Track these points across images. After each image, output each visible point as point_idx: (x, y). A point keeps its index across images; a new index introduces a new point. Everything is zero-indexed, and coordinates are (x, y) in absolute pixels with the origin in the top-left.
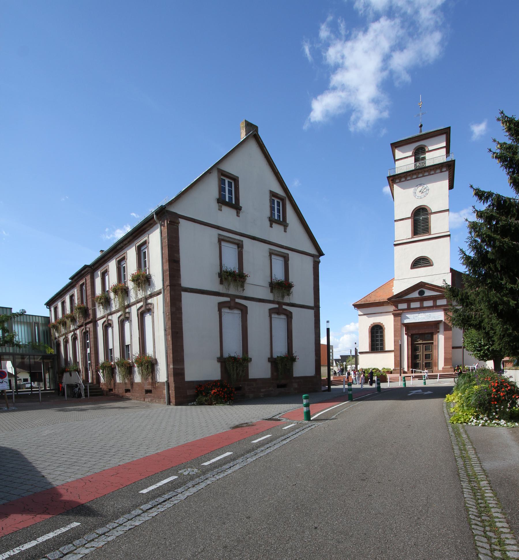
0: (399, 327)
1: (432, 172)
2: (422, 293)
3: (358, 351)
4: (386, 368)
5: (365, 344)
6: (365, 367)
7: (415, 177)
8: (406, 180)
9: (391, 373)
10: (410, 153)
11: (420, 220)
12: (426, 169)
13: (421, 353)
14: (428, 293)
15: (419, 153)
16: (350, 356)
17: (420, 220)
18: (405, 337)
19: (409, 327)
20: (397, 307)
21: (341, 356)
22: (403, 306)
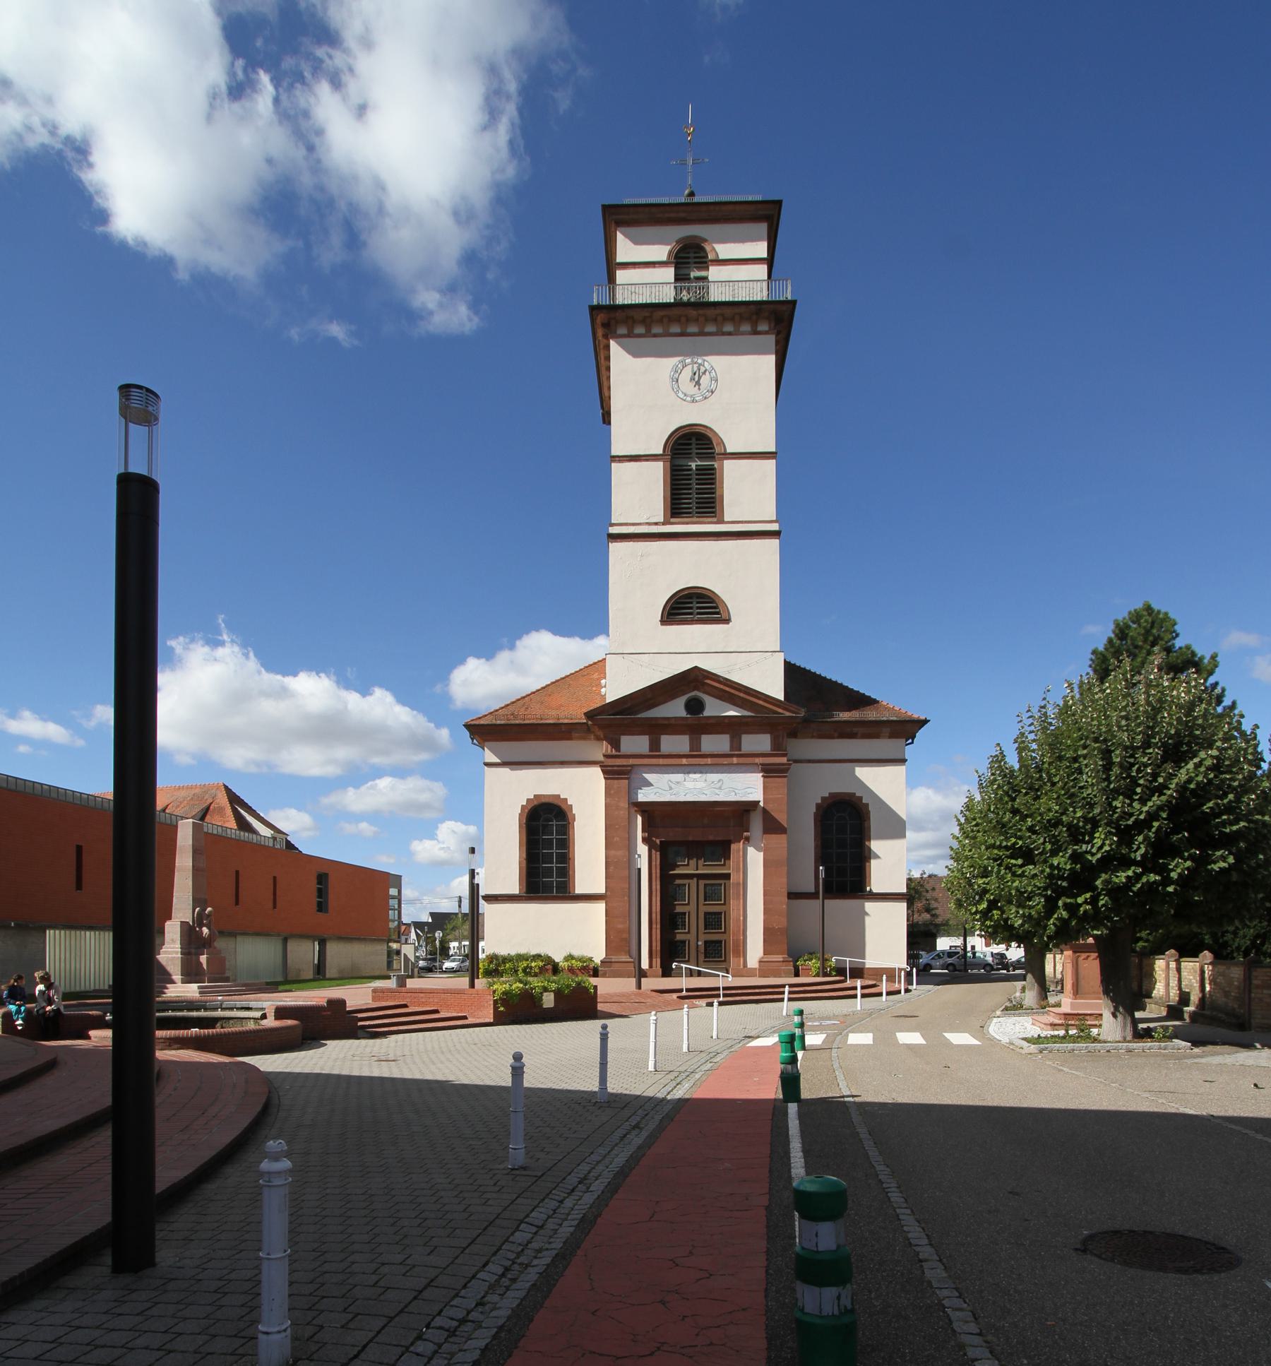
0: (623, 813)
1: (728, 328)
2: (695, 706)
3: (482, 892)
4: (576, 953)
5: (503, 867)
6: (503, 951)
7: (675, 329)
8: (648, 334)
9: (596, 973)
10: (660, 252)
11: (692, 469)
12: (711, 312)
13: (691, 906)
14: (715, 708)
15: (689, 258)
16: (456, 914)
17: (692, 469)
18: (643, 849)
20: (616, 744)
21: (432, 914)
22: (635, 744)
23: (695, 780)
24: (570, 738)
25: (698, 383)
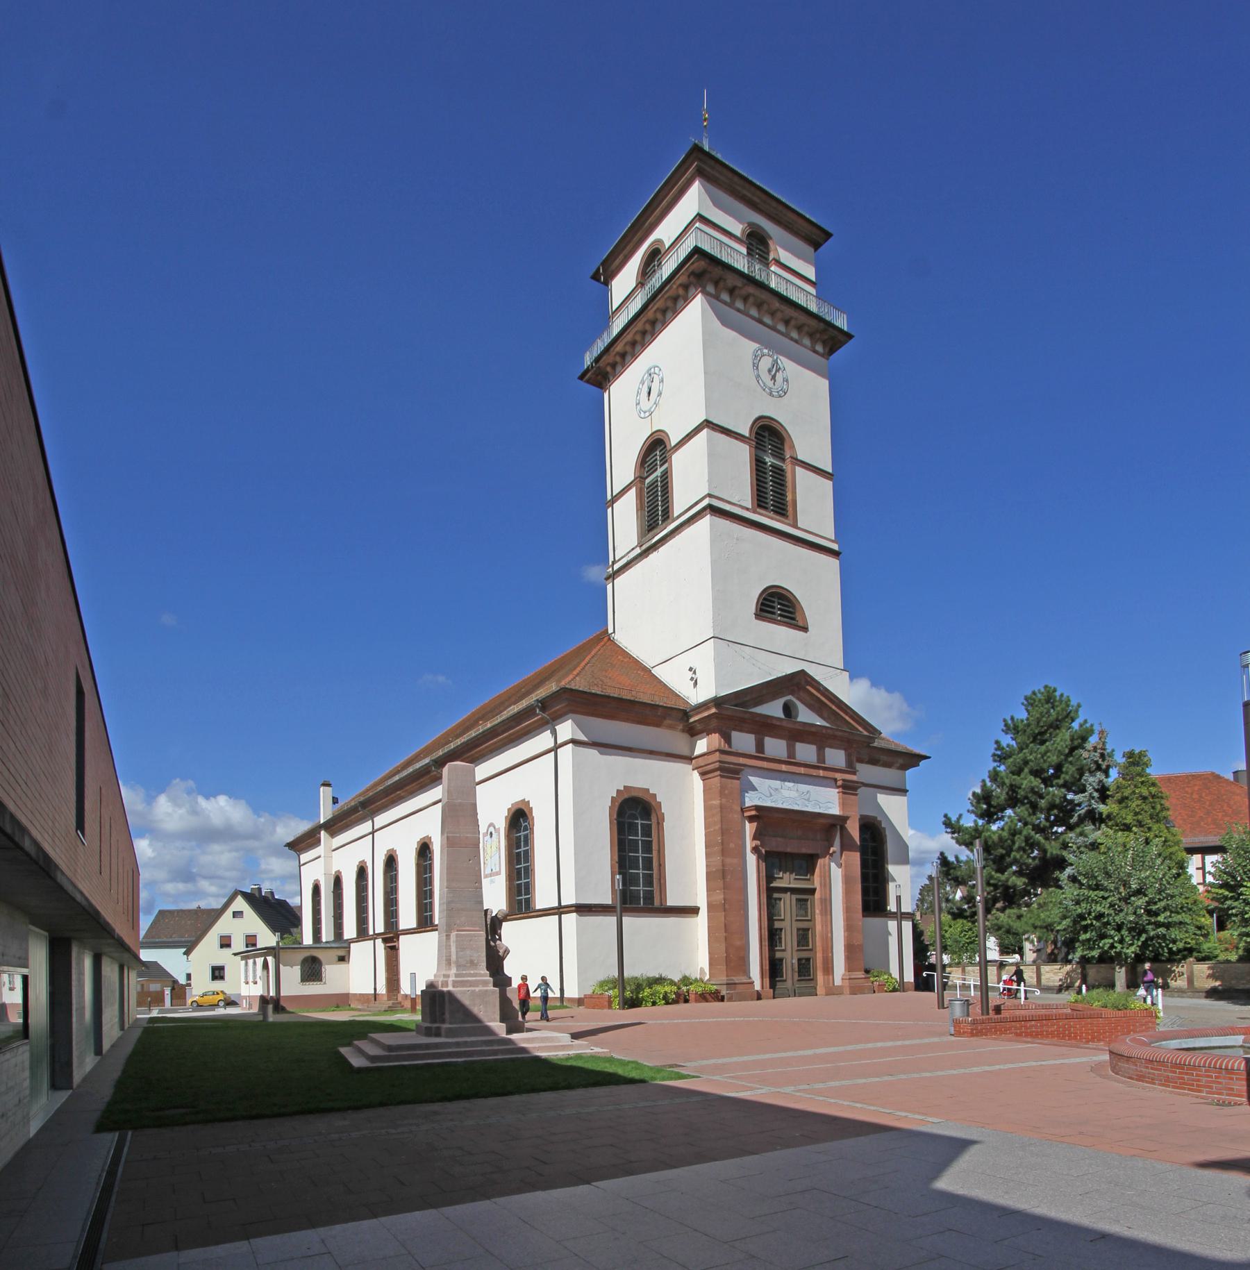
14: (806, 716)
18: (751, 859)
19: (765, 818)
20: (728, 739)
22: (744, 741)
23: (789, 789)
24: (658, 725)
25: (774, 378)
